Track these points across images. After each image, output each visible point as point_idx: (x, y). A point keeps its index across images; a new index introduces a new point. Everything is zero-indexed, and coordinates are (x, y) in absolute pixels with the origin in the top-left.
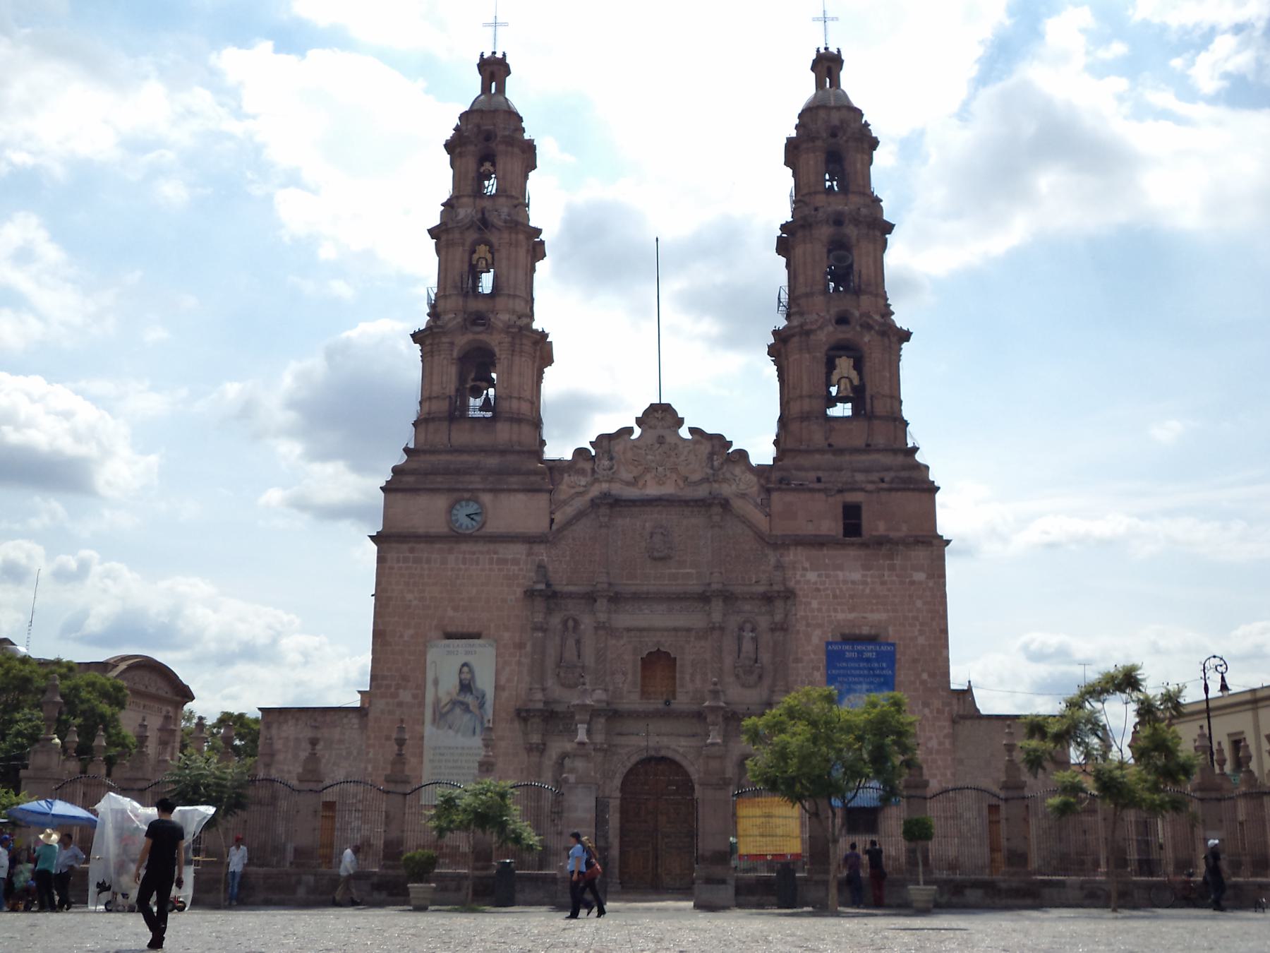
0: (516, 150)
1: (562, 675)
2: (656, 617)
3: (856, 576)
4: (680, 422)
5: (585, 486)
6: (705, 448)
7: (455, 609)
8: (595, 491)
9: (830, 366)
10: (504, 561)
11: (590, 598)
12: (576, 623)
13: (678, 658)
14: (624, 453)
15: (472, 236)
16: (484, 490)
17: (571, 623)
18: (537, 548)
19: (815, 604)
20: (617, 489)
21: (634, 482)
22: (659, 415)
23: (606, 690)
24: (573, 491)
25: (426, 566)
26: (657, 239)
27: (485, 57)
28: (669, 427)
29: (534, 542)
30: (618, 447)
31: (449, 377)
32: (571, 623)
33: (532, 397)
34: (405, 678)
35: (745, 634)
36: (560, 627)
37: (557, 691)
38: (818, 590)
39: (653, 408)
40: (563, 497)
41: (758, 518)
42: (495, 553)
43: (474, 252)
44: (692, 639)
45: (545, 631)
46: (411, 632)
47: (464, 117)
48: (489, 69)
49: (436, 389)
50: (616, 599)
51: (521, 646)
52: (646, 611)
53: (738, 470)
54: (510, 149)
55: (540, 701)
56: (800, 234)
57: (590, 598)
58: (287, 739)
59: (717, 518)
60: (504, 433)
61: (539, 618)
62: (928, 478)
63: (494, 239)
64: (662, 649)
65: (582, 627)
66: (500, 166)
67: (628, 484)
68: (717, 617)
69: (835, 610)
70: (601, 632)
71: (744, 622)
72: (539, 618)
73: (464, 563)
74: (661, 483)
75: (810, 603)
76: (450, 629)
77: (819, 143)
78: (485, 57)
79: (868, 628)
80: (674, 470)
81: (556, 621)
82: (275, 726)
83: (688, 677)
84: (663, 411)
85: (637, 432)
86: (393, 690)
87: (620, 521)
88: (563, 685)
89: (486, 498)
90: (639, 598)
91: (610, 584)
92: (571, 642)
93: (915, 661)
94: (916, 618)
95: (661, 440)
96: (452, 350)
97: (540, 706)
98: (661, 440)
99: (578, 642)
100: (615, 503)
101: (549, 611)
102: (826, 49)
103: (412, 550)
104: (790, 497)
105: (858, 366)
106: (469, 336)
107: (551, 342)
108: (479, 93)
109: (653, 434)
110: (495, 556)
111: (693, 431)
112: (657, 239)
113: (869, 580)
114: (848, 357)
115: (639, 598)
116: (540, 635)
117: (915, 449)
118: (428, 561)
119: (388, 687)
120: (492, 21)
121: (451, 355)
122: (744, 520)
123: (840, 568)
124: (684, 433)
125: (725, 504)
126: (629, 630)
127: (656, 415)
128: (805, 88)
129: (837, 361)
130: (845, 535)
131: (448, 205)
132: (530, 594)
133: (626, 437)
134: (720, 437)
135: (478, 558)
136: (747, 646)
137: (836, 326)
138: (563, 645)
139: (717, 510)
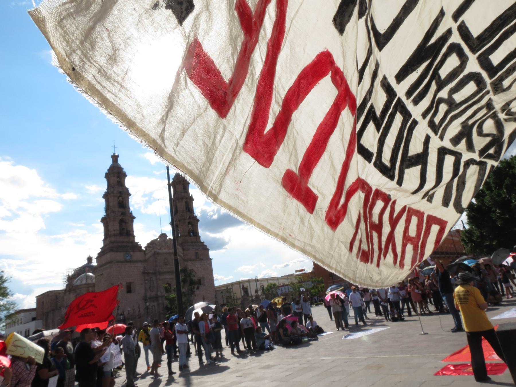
8: (153, 251)
15: (119, 195)
17: (151, 279)
20: (157, 250)
21: (160, 249)
41: (182, 255)
50: (160, 273)
57: (155, 273)
67: (158, 249)
89: (132, 253)
95: (164, 240)
98: (164, 240)
100: (158, 254)
103: (118, 265)
124: (168, 238)
126: (162, 279)
132: (144, 273)
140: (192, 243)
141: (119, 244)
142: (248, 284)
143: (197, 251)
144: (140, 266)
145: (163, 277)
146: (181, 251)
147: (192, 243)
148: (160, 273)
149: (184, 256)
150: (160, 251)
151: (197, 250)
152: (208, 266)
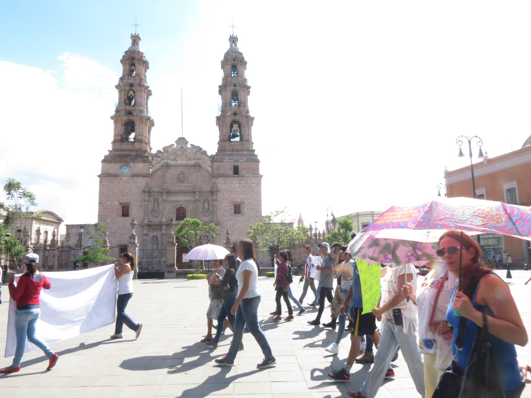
0: (141, 63)
1: (153, 214)
2: (181, 198)
3: (237, 185)
4: (188, 142)
5: (160, 161)
6: (194, 150)
7: (122, 196)
8: (163, 162)
9: (231, 126)
10: (137, 182)
11: (161, 193)
12: (158, 200)
13: (187, 209)
14: (171, 151)
16: (131, 162)
17: (156, 200)
18: (145, 179)
19: (225, 193)
22: (182, 141)
23: (166, 218)
24: (157, 162)
25: (114, 184)
26: (181, 90)
27: (133, 35)
28: (184, 144)
29: (145, 177)
30: (170, 150)
31: (122, 129)
32: (156, 200)
33: (146, 136)
34: (108, 216)
35: (205, 202)
36: (153, 201)
37: (152, 218)
38: (226, 189)
39: (180, 139)
40: (153, 164)
42: (134, 180)
43: (129, 93)
44: (191, 203)
45: (149, 202)
46: (110, 203)
47: (126, 52)
48: (134, 38)
49: (117, 133)
50: (169, 193)
51: (141, 206)
52: (177, 196)
53: (204, 156)
54: (139, 62)
55: (147, 221)
56: (224, 89)
57: (161, 193)
58: (74, 233)
59: (197, 170)
60: (137, 146)
61: (147, 198)
62: (257, 158)
63: (134, 89)
64: (182, 206)
65: (159, 200)
66: (136, 67)
67: (173, 160)
68: (197, 197)
69: (231, 195)
70: (165, 202)
71: (205, 199)
72: (147, 198)
73: (125, 183)
74: (182, 159)
75: (223, 193)
76: (121, 202)
77: (230, 62)
78: (133, 35)
79: (240, 200)
80: (186, 156)
81: (151, 199)
82: (70, 230)
83: (189, 214)
84: (182, 140)
85: (175, 145)
86: (104, 219)
87: (170, 171)
88: (154, 217)
90: (177, 193)
91: (167, 189)
92: (156, 205)
93: (253, 209)
94: (253, 197)
95: (182, 147)
96: (122, 122)
97: (147, 223)
98: (182, 147)
99: (158, 204)
101: (150, 196)
102: (233, 35)
103: (110, 179)
104: (218, 164)
105: (240, 127)
106: (127, 118)
107: (153, 120)
108: (131, 45)
109: (180, 146)
110: (134, 181)
111: (191, 145)
112: (181, 90)
113: (240, 187)
114: (237, 124)
115: (177, 193)
116: (147, 203)
117: (254, 151)
118: (115, 182)
119: (103, 218)
120: (135, 24)
121: (122, 123)
122: (206, 170)
123: (232, 183)
124: (189, 146)
125: (200, 166)
126: (173, 201)
127: (181, 141)
128: (226, 46)
129: (234, 125)
130: (234, 174)
131: (121, 79)
132: (144, 192)
133: (172, 147)
134: (199, 147)
135: (129, 182)
136: (206, 205)
137: (233, 116)
138: (154, 206)
139: (197, 167)
140: (233, 151)
141: (126, 153)
142: (371, 218)
143: (236, 164)
144: (141, 182)
145: (174, 198)
146: (209, 163)
147: (233, 151)
148: (169, 193)
149: (212, 170)
150: (173, 163)
151: (237, 161)
152: (253, 185)
